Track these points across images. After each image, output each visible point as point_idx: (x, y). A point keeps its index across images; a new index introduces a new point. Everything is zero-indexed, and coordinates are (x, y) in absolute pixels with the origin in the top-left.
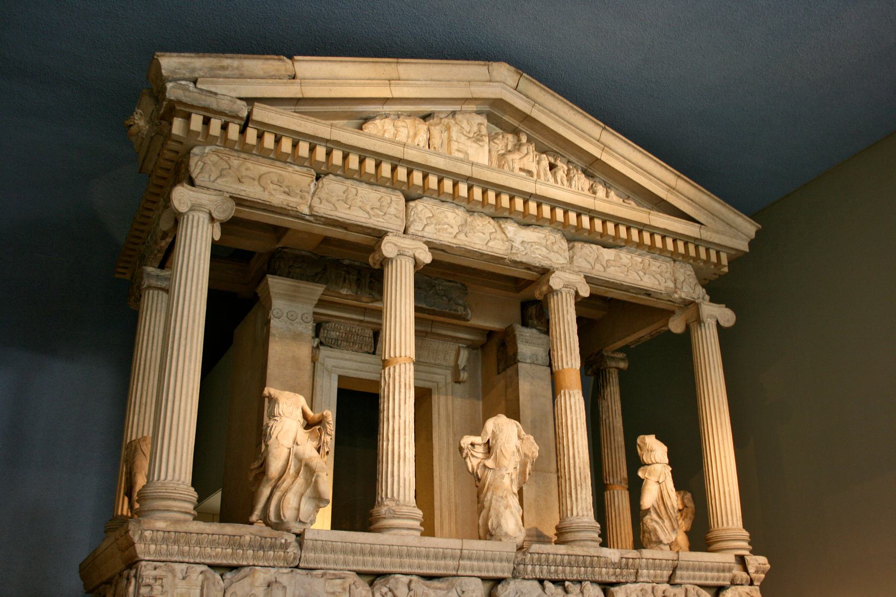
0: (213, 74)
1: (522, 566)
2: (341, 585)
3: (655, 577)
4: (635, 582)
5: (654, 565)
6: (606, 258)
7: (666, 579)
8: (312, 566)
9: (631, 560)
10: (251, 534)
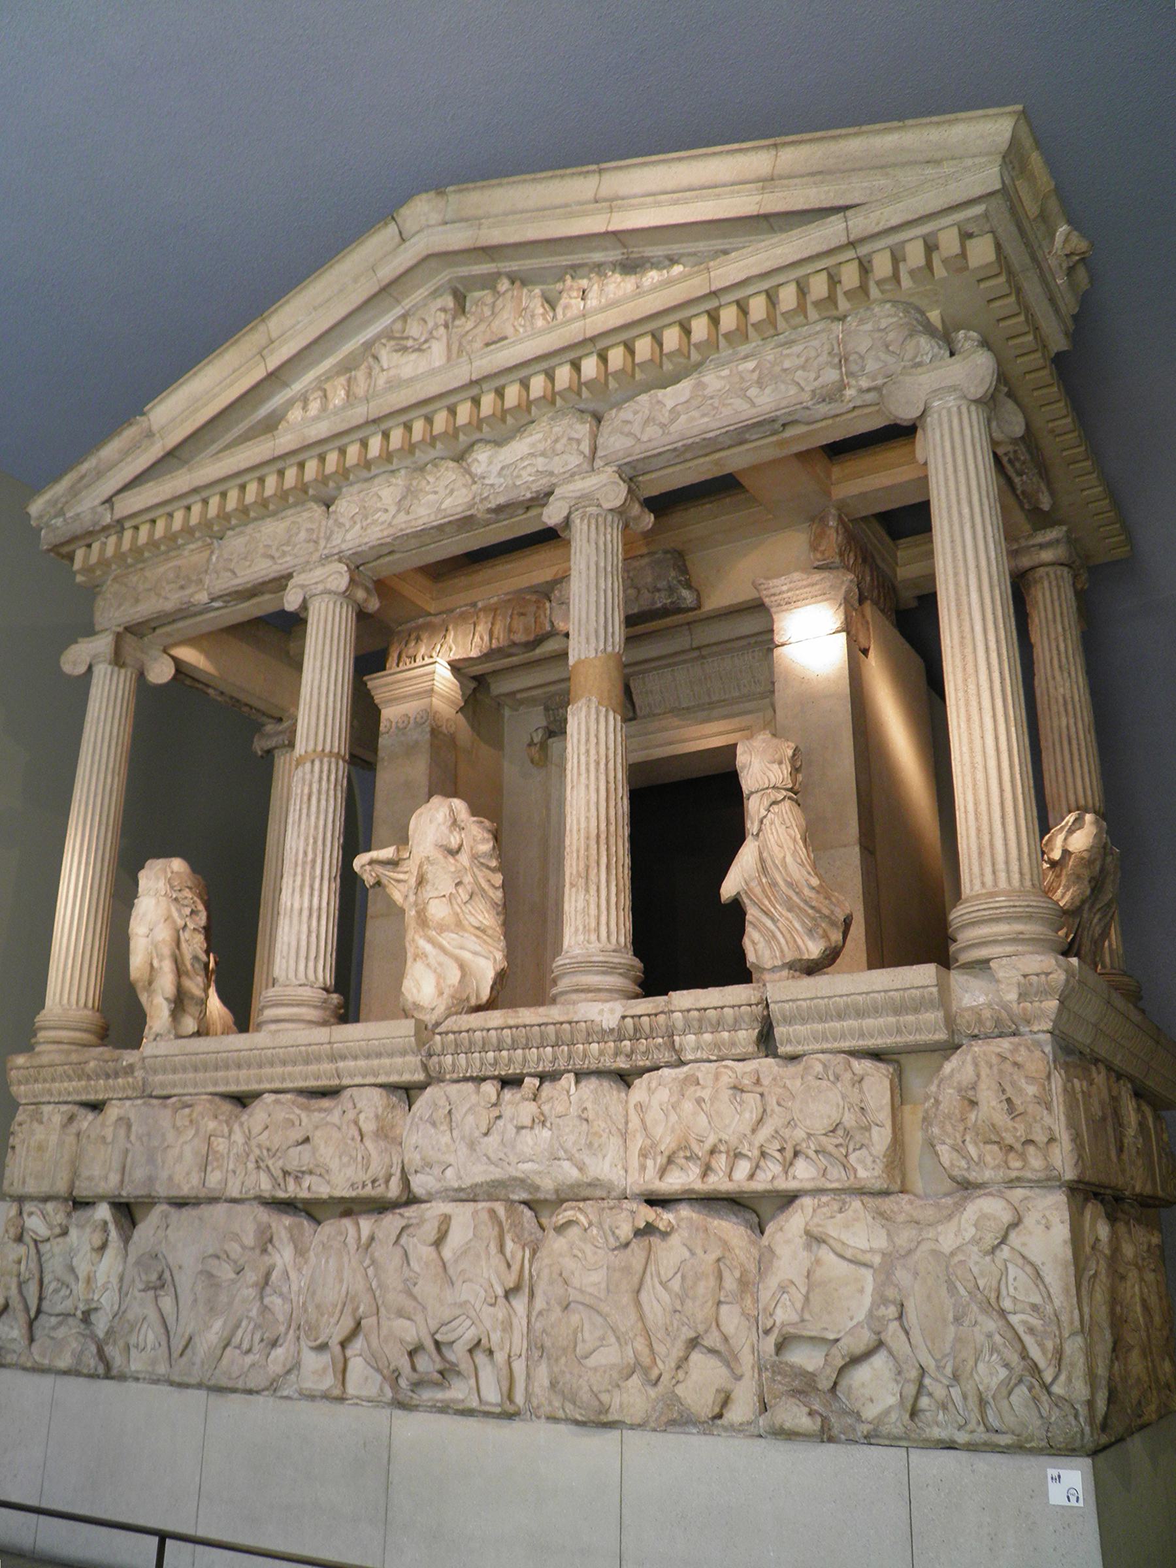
0: (74, 492)
1: (435, 1059)
2: (190, 1115)
3: (717, 1045)
4: (681, 1063)
5: (700, 1022)
6: (670, 404)
7: (752, 1048)
8: (164, 1093)
9: (645, 1019)
10: (95, 1059)
